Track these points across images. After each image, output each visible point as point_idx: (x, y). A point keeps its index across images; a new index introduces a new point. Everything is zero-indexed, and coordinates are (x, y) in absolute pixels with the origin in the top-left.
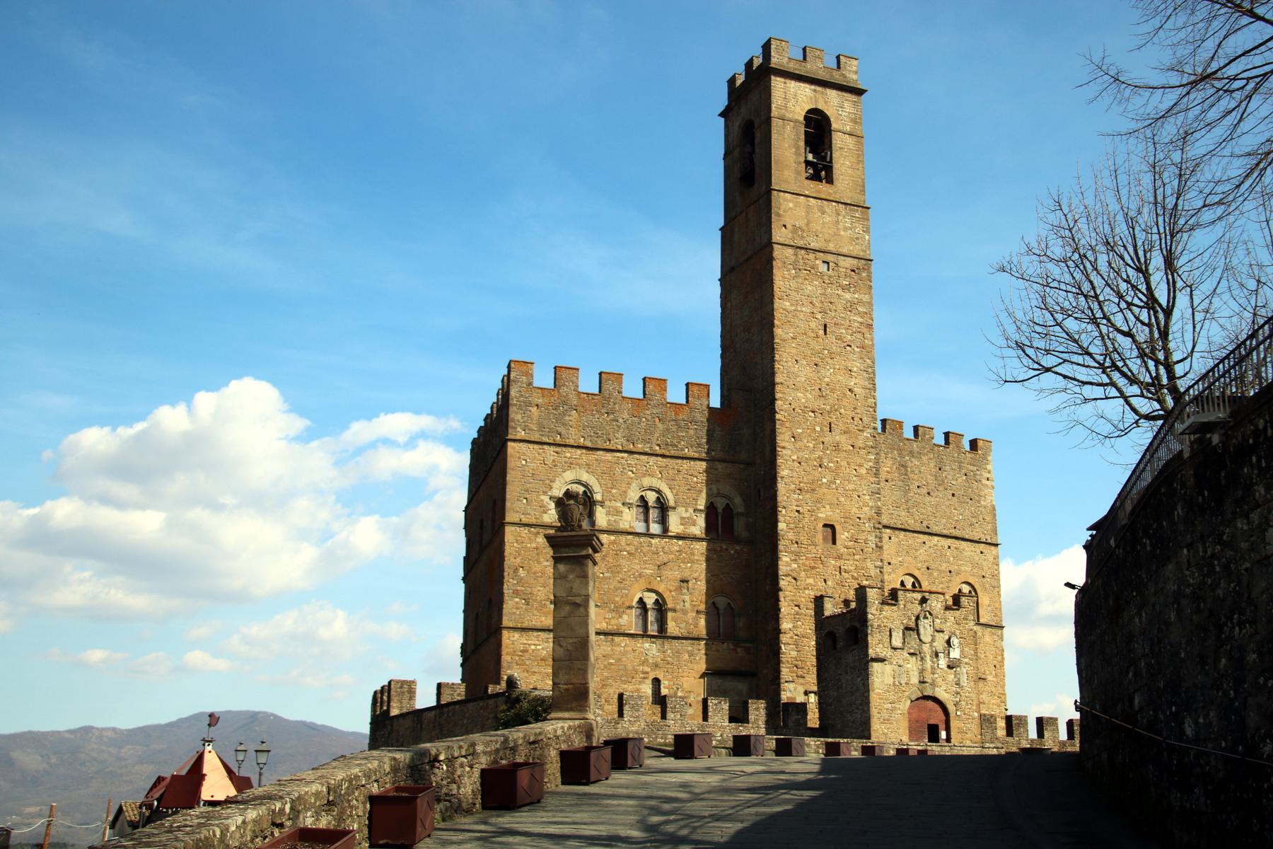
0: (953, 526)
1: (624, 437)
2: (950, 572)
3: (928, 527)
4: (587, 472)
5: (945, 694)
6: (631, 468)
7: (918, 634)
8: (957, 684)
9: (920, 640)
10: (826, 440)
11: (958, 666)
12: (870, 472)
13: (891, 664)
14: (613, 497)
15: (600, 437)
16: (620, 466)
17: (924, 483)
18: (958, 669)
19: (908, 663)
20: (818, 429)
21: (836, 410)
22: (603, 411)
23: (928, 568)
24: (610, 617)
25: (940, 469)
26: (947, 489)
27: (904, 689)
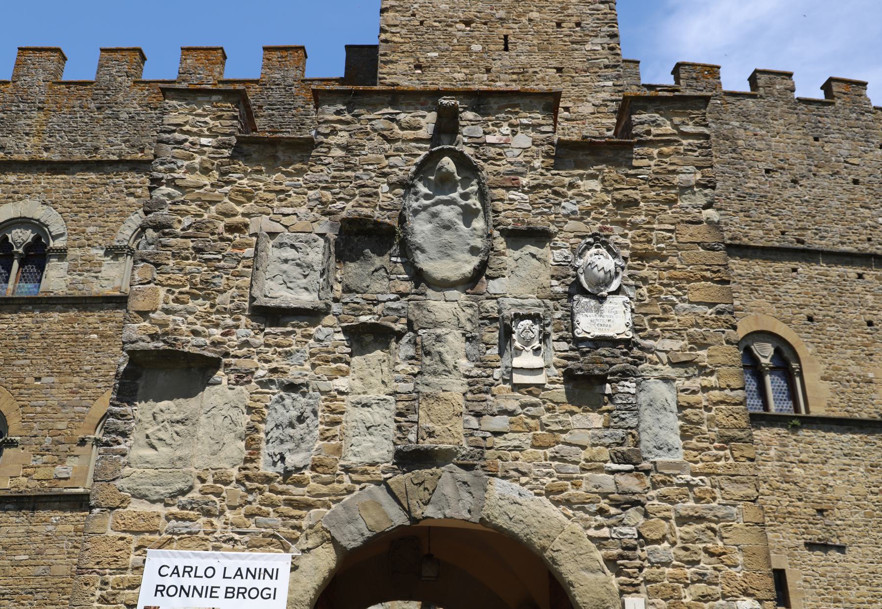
0: (864, 237)
1: (128, 141)
2: (870, 324)
3: (803, 242)
4: (44, 203)
5: (556, 512)
6: (132, 190)
7: (407, 250)
8: (624, 459)
9: (419, 277)
10: (496, 66)
11: (625, 374)
12: (602, 109)
13: (242, 377)
14: (88, 240)
15: (81, 146)
16: (111, 188)
17: (782, 164)
18: (629, 386)
19: (344, 374)
20: (476, 47)
21: (519, 16)
22: (92, 106)
23: (810, 319)
24: (39, 463)
25: (816, 139)
26: (837, 173)
27: (297, 492)
